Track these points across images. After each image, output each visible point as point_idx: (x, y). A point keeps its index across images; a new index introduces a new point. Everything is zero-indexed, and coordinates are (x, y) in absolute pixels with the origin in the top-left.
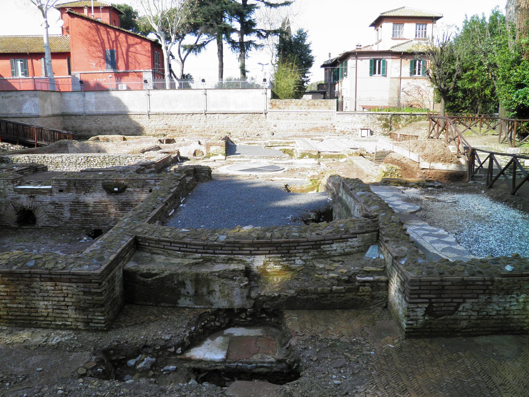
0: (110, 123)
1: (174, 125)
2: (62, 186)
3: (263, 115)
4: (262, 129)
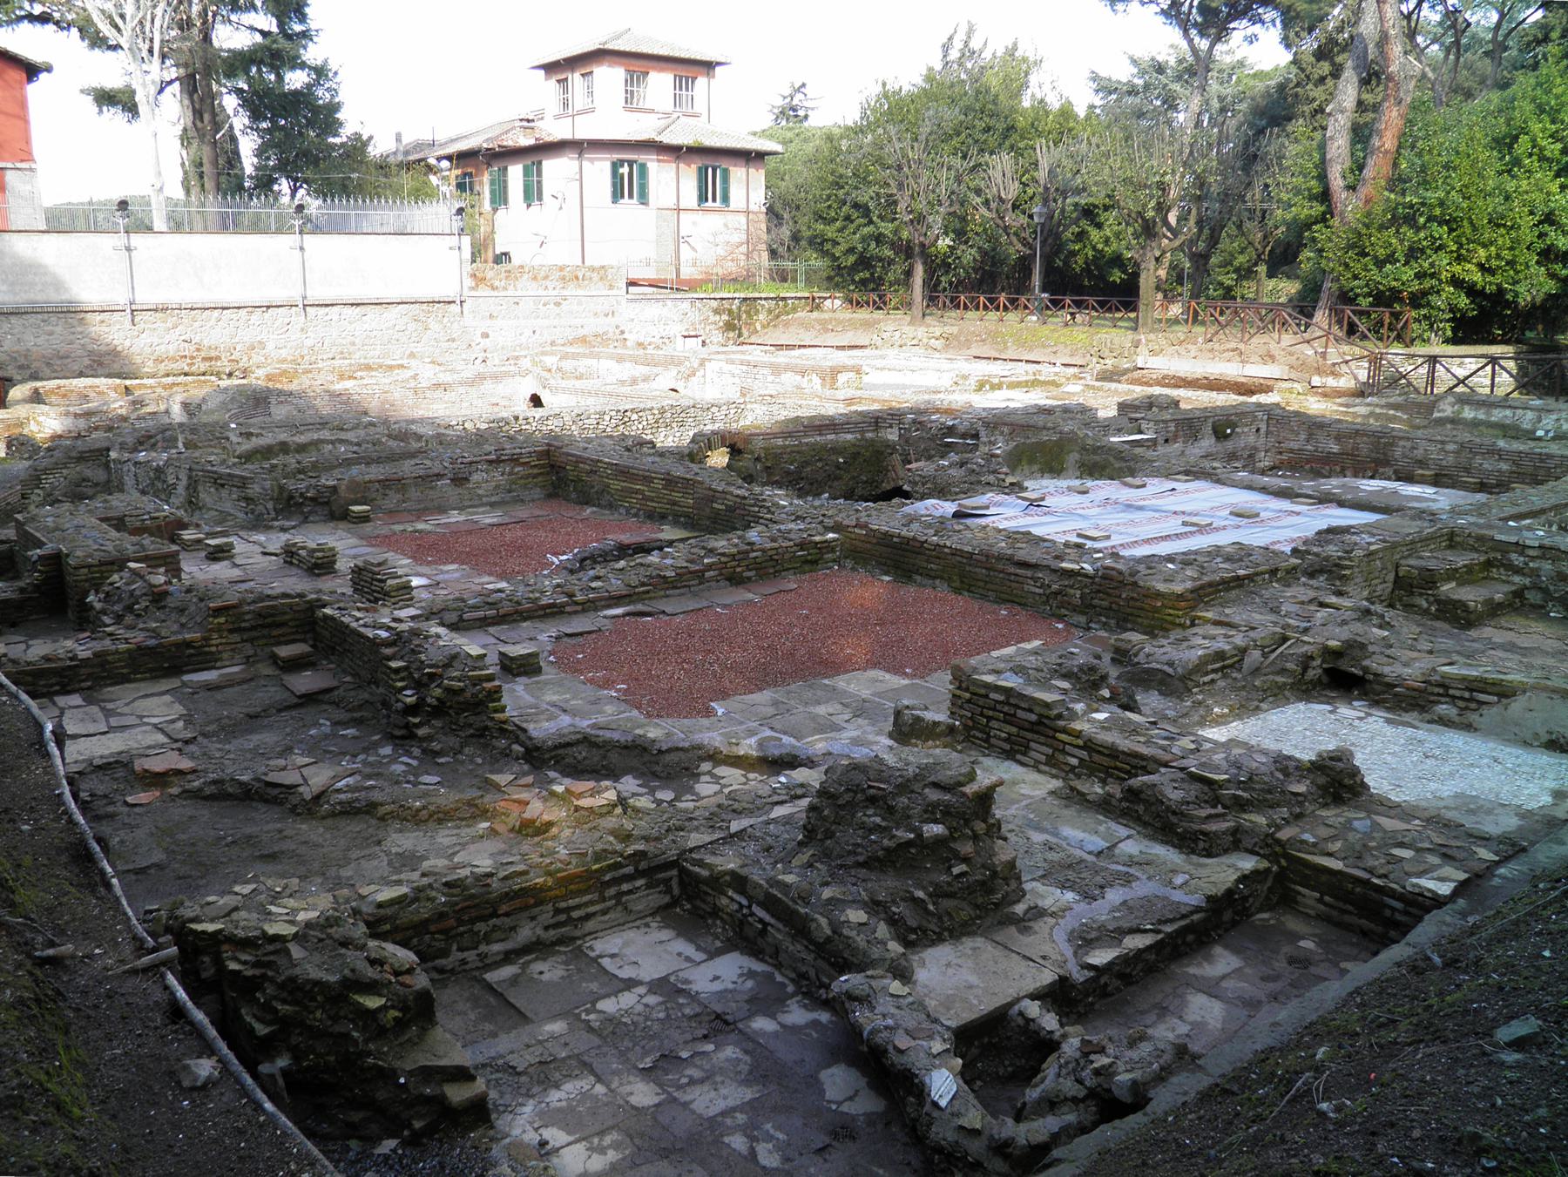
1: (213, 343)
3: (455, 308)
4: (454, 345)
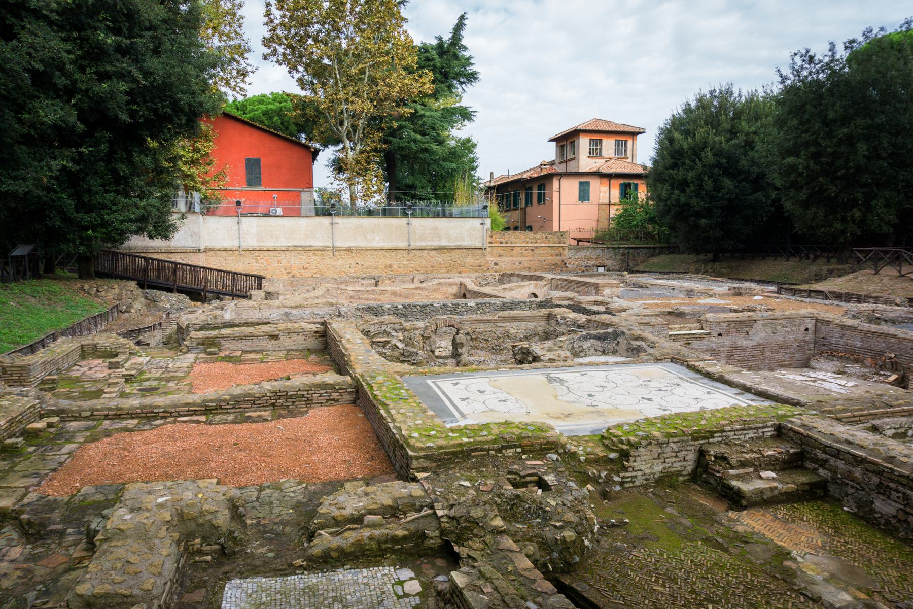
0: (279, 262)
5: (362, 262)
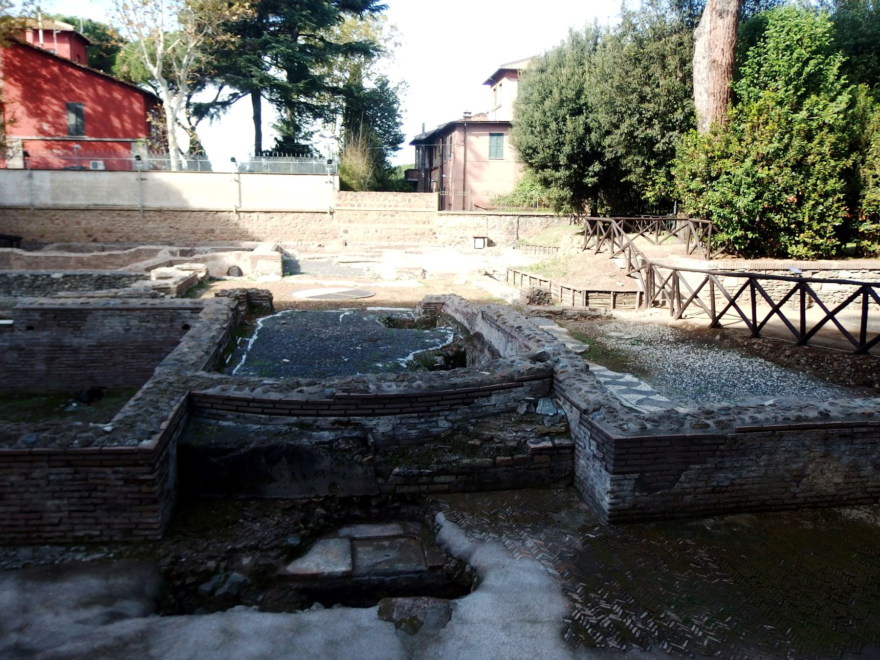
0: (78, 223)
2: (31, 320)
4: (326, 236)
5: (178, 226)
